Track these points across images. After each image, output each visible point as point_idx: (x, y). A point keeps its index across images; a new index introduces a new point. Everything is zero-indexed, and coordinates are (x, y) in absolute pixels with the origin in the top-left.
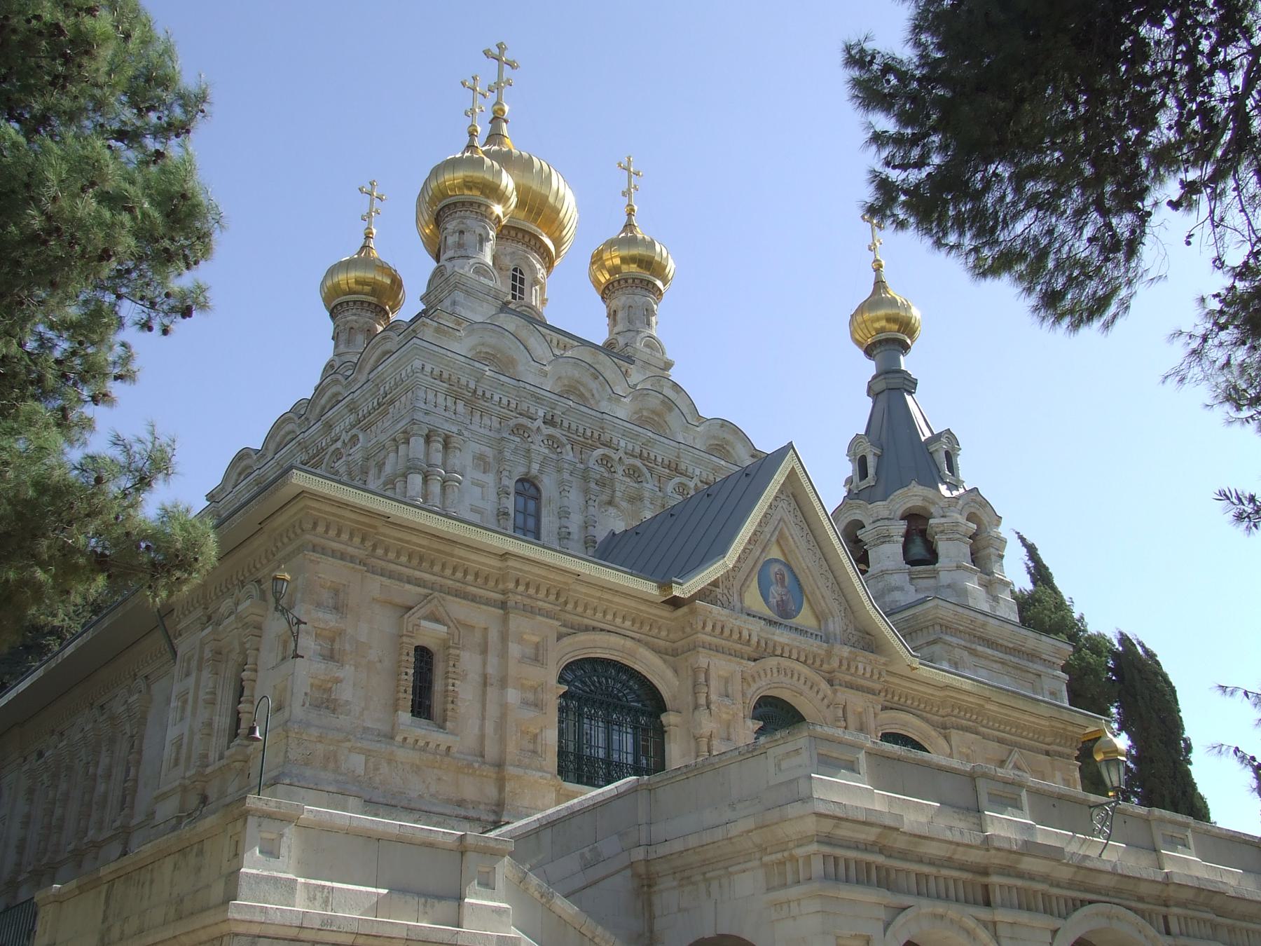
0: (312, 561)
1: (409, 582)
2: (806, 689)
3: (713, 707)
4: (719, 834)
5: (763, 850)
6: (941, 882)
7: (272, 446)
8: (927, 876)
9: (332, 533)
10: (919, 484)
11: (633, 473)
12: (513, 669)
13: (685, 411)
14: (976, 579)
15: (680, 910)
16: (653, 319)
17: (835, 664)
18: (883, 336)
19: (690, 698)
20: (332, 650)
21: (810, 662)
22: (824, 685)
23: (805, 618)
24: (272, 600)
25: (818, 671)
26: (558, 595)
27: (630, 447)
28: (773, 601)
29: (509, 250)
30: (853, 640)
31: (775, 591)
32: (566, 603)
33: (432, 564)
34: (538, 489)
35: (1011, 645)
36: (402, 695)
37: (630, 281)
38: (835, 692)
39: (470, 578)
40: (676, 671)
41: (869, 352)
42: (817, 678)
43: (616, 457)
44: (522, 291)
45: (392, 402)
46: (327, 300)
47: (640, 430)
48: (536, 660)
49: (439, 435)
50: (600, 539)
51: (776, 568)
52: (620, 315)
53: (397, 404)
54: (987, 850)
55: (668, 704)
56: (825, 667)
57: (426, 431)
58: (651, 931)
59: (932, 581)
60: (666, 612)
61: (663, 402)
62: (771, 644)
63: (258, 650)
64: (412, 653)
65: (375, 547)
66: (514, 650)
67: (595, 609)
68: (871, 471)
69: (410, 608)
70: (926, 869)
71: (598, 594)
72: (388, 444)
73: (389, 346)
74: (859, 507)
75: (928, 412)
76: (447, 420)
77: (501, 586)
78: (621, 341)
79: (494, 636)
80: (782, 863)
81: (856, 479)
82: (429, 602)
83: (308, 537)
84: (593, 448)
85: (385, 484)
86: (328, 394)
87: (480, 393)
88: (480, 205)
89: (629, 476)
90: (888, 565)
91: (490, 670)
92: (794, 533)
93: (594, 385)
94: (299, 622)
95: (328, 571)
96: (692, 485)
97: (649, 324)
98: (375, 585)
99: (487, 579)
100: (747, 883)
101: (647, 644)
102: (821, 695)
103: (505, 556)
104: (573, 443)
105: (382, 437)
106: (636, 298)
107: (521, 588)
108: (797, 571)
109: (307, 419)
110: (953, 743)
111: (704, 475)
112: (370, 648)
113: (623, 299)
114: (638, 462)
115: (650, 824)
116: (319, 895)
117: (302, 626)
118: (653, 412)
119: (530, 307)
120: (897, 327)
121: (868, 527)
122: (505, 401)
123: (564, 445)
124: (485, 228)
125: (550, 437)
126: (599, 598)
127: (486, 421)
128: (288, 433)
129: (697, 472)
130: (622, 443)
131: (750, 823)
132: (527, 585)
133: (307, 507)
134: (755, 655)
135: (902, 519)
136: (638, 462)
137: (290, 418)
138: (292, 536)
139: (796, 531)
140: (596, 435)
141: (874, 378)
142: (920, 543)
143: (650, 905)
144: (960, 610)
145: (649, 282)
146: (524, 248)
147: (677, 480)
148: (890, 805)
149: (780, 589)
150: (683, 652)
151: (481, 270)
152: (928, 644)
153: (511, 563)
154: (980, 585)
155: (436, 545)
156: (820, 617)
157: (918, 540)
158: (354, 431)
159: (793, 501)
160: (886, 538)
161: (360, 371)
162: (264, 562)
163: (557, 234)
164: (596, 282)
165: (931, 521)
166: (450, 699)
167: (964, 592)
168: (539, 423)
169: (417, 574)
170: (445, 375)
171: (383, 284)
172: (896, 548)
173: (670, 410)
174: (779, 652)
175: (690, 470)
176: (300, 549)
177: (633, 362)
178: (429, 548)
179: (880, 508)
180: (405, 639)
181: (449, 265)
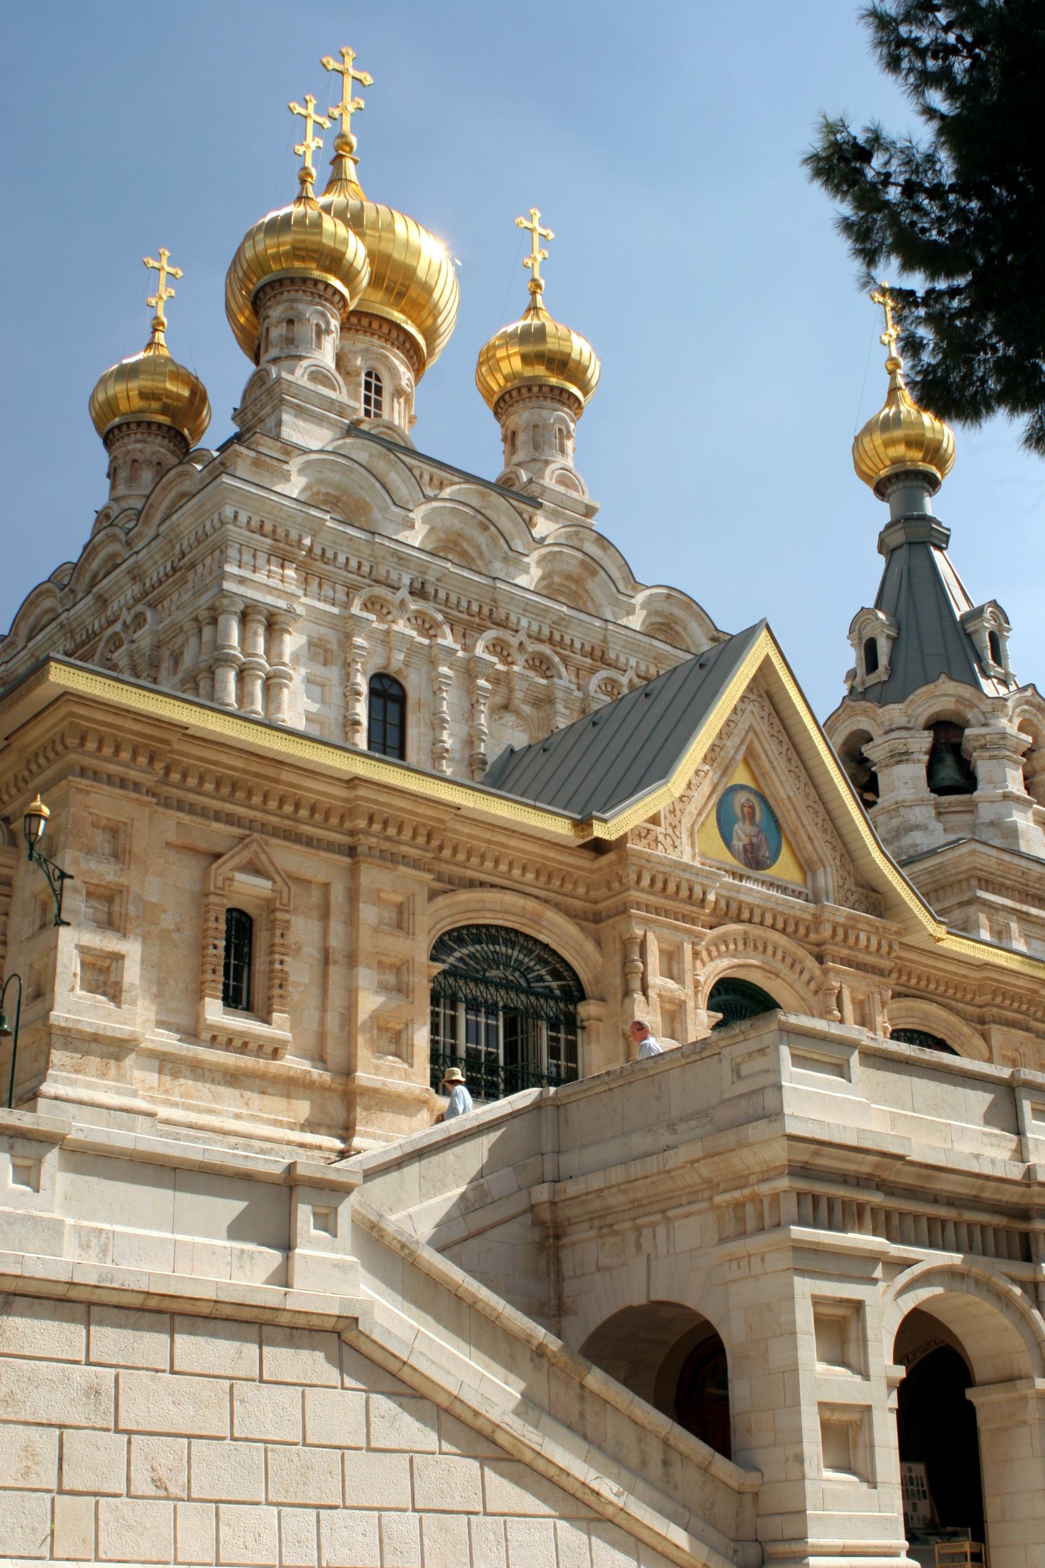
0: (79, 790)
1: (217, 819)
2: (783, 969)
3: (651, 993)
4: (652, 1164)
5: (713, 1186)
6: (964, 1231)
7: (24, 630)
8: (943, 1222)
9: (108, 751)
10: (951, 679)
11: (541, 665)
12: (366, 941)
13: (616, 575)
14: (1030, 814)
15: (599, 1269)
16: (569, 444)
17: (827, 932)
18: (899, 468)
19: (618, 981)
20: (110, 914)
21: (790, 929)
22: (811, 963)
23: (784, 868)
24: (24, 846)
25: (802, 941)
26: (429, 837)
27: (535, 627)
28: (738, 844)
29: (360, 346)
30: (853, 899)
31: (742, 832)
32: (441, 848)
33: (250, 793)
34: (402, 688)
36: (209, 976)
37: (535, 389)
38: (825, 972)
39: (303, 813)
40: (598, 943)
41: (881, 489)
42: (801, 953)
43: (514, 641)
44: (378, 405)
45: (192, 566)
46: (99, 422)
47: (550, 603)
48: (399, 926)
49: (259, 613)
50: (491, 760)
51: (741, 798)
52: (521, 438)
53: (200, 568)
54: (1028, 1186)
55: (588, 989)
56: (813, 936)
57: (241, 607)
58: (559, 1298)
59: (967, 817)
60: (584, 861)
61: (583, 564)
62: (734, 906)
63: (7, 914)
64: (223, 918)
65: (168, 770)
66: (368, 914)
67: (483, 857)
68: (883, 660)
69: (218, 856)
70: (943, 1212)
71: (487, 835)
72: (188, 625)
73: (187, 486)
74: (864, 712)
75: (965, 575)
76: (271, 590)
77: (347, 825)
78: (524, 476)
79: (338, 894)
80: (739, 1206)
81: (861, 671)
82: (247, 846)
83: (74, 757)
84: (481, 629)
85: (183, 682)
86: (103, 554)
87: (317, 551)
88: (316, 282)
89: (533, 667)
90: (906, 794)
91: (334, 942)
92: (770, 750)
93: (481, 539)
94: (63, 875)
95: (102, 803)
96: (624, 680)
97: (562, 450)
98: (170, 823)
99: (327, 815)
100: (691, 1230)
101: (557, 906)
102: (806, 976)
103: (354, 782)
104: (452, 623)
105: (178, 616)
106: (545, 413)
107: (377, 827)
108: (772, 803)
109: (72, 591)
110: (994, 1043)
111: (643, 667)
112: (164, 911)
113: (526, 415)
114: (546, 649)
115: (558, 1152)
116: (94, 1241)
117: (67, 881)
118: (569, 577)
119: (390, 427)
120: (920, 455)
121: (877, 741)
122: (353, 564)
123: (435, 625)
124: (323, 315)
125: (419, 615)
126: (489, 841)
127: (327, 591)
128: (46, 612)
129: (633, 662)
130: (524, 623)
131: (696, 1151)
132: (386, 823)
133: (72, 714)
134: (713, 920)
135: (927, 727)
136: (546, 649)
137: (48, 591)
138: (51, 755)
139: (772, 747)
140: (486, 610)
141: (888, 527)
142: (952, 764)
143: (558, 1261)
144: (1006, 857)
145: (563, 390)
146: (382, 343)
147: (603, 674)
148: (894, 1126)
149: (748, 828)
150: (609, 917)
151: (318, 376)
152: (961, 904)
153: (361, 792)
154: (1036, 822)
155: (254, 767)
156: (806, 867)
157: (949, 760)
158: (139, 608)
159: (767, 704)
160: (901, 757)
161: (146, 521)
162: (13, 791)
163: (429, 321)
164: (487, 392)
165: (967, 732)
166: (277, 982)
167: (1013, 832)
168: (403, 593)
169: (229, 808)
170: (268, 527)
171: (178, 397)
172: (919, 770)
173: (594, 573)
174: (746, 915)
175: (622, 659)
176: (62, 776)
177: (540, 506)
178: (244, 771)
179: (894, 712)
180: (213, 899)
181: (274, 371)
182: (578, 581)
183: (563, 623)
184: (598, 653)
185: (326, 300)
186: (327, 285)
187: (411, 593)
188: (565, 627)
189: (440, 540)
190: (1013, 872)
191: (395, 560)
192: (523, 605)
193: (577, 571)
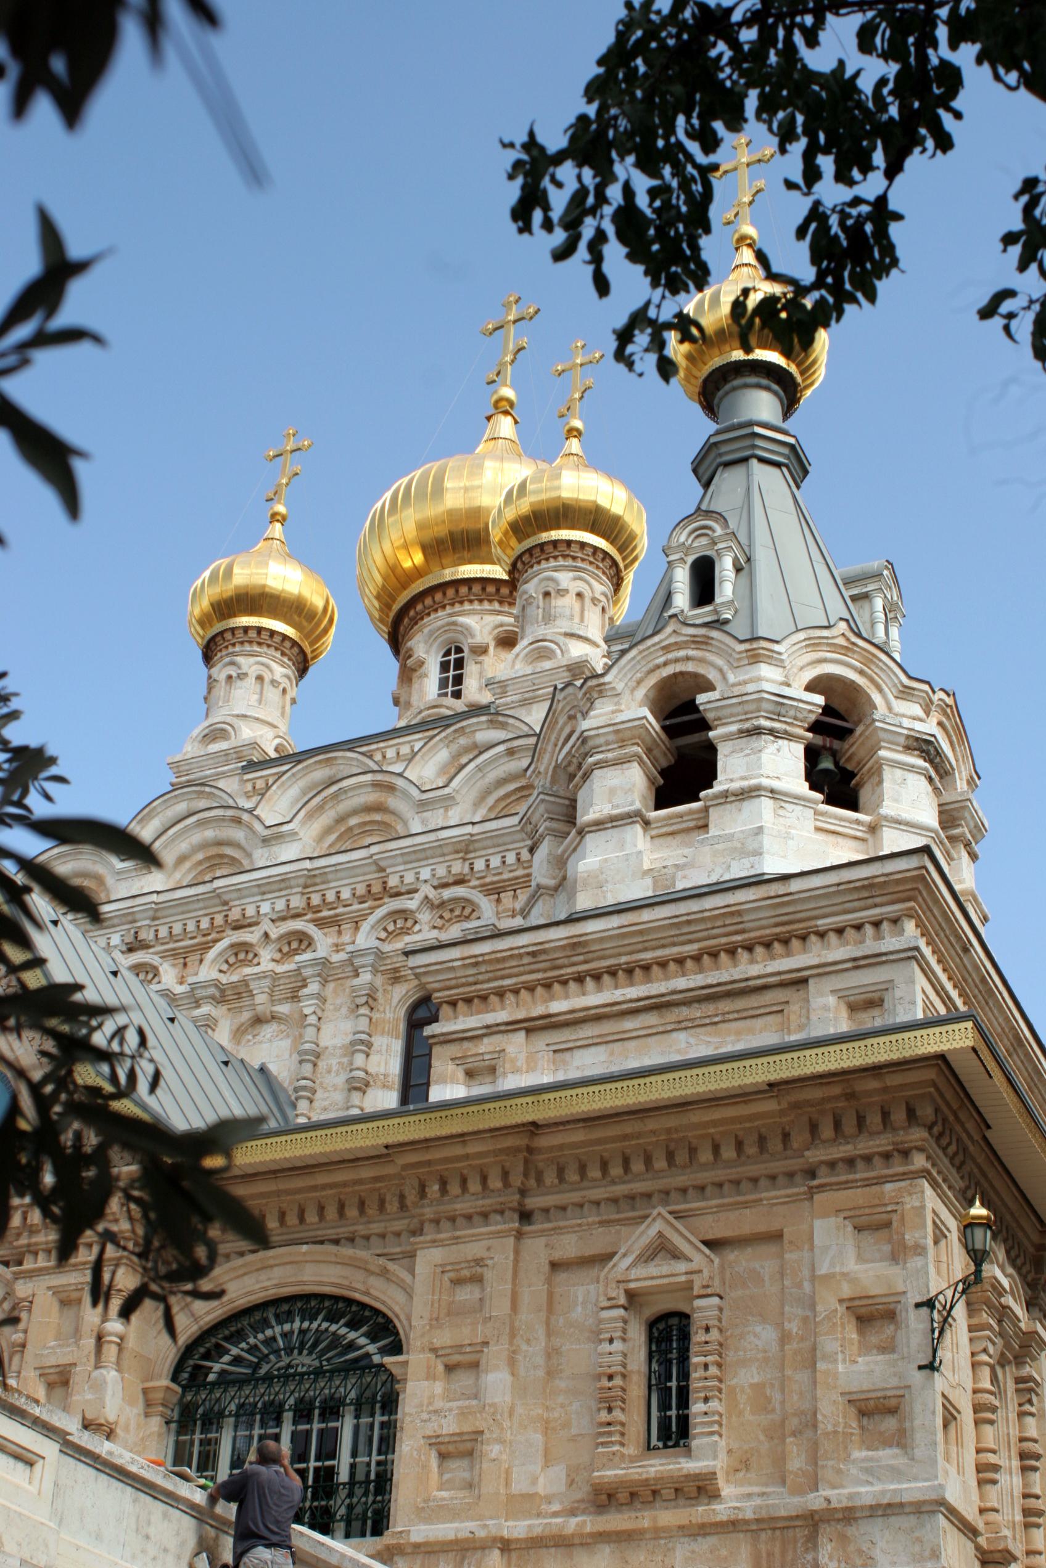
27: (280, 905)
35: (692, 948)
129: (425, 873)
146: (457, 608)
147: (380, 912)
175: (409, 878)
182: (379, 808)
183: (318, 880)
184: (376, 888)
185: (242, 643)
186: (233, 630)
187: (131, 950)
188: (324, 883)
189: (200, 863)
190: (514, 963)
192: (256, 890)
193: (371, 797)
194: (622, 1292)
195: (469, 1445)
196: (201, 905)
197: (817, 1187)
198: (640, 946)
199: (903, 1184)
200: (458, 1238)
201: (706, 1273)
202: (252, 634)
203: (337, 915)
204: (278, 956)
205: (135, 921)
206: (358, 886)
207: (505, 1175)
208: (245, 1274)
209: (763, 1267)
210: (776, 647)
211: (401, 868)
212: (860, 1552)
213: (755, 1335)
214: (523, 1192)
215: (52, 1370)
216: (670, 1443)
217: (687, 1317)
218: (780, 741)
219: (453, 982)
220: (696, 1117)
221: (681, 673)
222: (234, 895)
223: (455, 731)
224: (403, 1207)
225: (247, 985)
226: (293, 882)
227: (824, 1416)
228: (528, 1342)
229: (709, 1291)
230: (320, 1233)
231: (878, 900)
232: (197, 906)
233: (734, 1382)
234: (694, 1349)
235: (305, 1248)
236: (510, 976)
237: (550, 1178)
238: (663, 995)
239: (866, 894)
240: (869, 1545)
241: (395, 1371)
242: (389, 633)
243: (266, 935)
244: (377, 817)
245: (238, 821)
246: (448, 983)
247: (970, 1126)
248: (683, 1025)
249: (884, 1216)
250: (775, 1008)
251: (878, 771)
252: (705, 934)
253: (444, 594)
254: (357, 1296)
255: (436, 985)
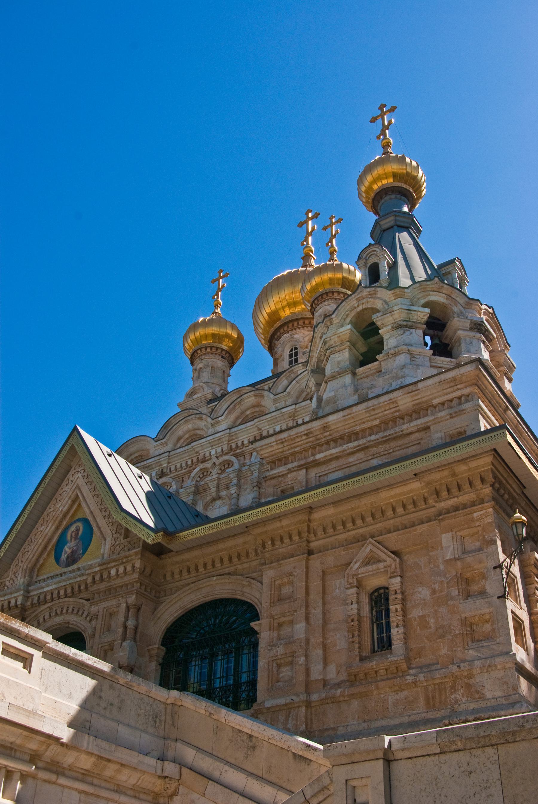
27: (219, 450)
35: (377, 422)
51: (73, 528)
61: (255, 395)
62: (42, 597)
114: (227, 457)
118: (254, 406)
146: (294, 331)
173: (262, 396)
182: (258, 405)
183: (234, 438)
188: (236, 438)
189: (187, 439)
190: (298, 440)
191: (146, 469)
192: (209, 445)
194: (355, 579)
195: (290, 659)
196: (187, 454)
197: (442, 519)
198: (353, 424)
199: (482, 512)
200: (281, 564)
201: (393, 566)
202: (209, 350)
203: (243, 451)
204: (220, 472)
205: (161, 465)
206: (251, 438)
207: (299, 534)
208: (190, 593)
209: (420, 561)
210: (406, 290)
211: (268, 427)
212: (477, 692)
213: (419, 593)
214: (308, 542)
215: (106, 644)
216: (384, 649)
217: (387, 588)
218: (411, 330)
219: (274, 452)
220: (384, 494)
221: (366, 309)
222: (200, 448)
223: (289, 372)
224: (257, 554)
225: (208, 485)
226: (224, 440)
227: (454, 626)
228: (315, 608)
229: (395, 574)
230: (221, 571)
231: (459, 387)
232: (185, 455)
233: (411, 616)
234: (390, 602)
235: (215, 578)
236: (297, 446)
237: (320, 533)
238: (365, 444)
239: (452, 384)
240: (481, 687)
241: (256, 628)
242: (269, 348)
243: (214, 463)
244: (258, 409)
245: (201, 419)
246: (271, 453)
247: (514, 486)
248: (375, 456)
249: (475, 529)
250: (416, 442)
251: (459, 341)
252: (382, 414)
253: (288, 327)
254: (239, 597)
255: (266, 455)
